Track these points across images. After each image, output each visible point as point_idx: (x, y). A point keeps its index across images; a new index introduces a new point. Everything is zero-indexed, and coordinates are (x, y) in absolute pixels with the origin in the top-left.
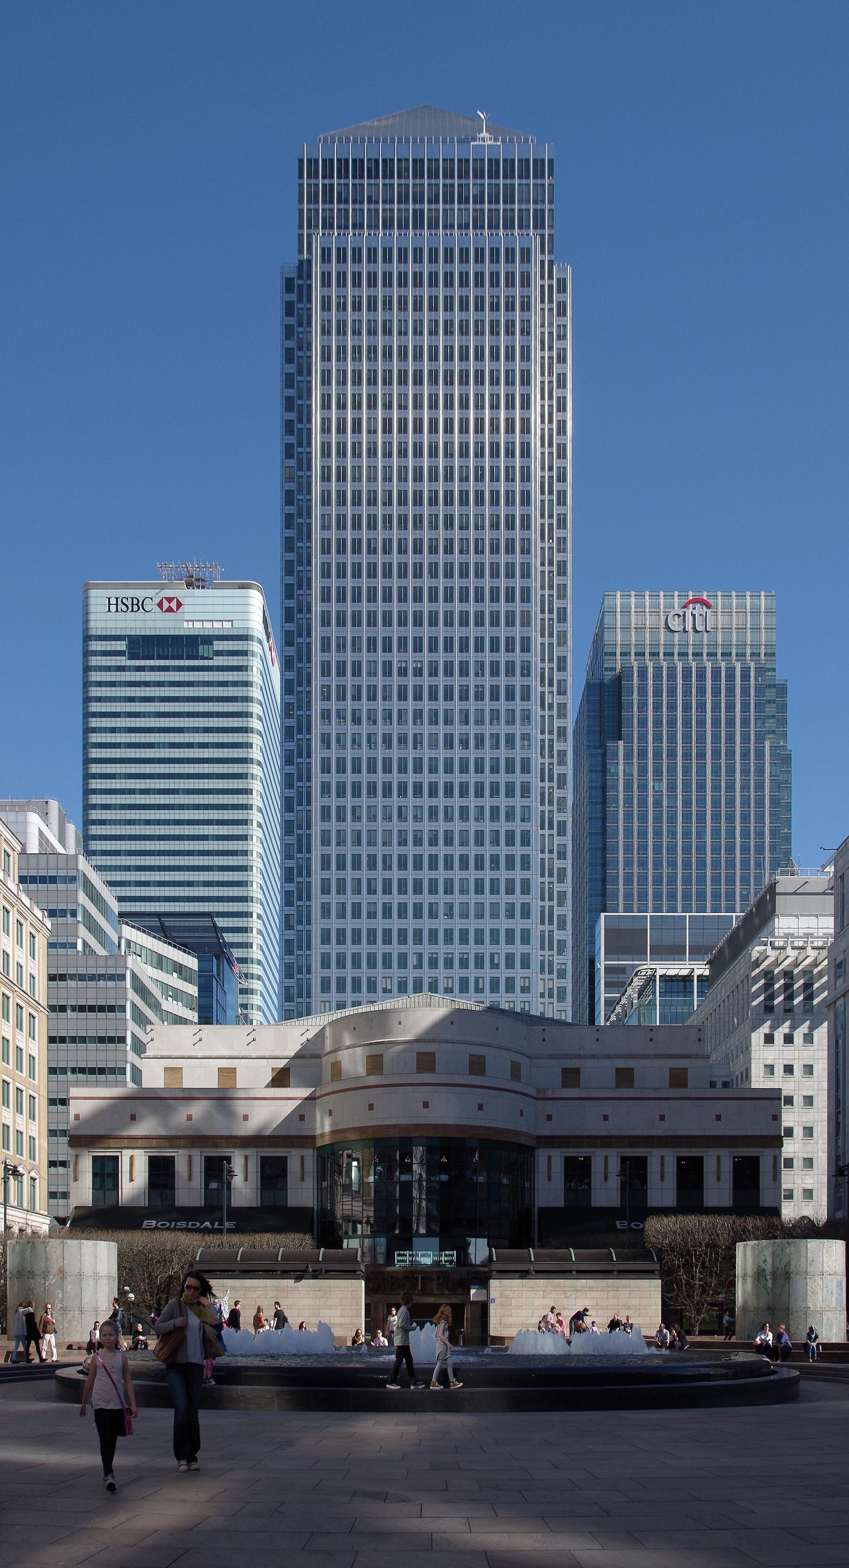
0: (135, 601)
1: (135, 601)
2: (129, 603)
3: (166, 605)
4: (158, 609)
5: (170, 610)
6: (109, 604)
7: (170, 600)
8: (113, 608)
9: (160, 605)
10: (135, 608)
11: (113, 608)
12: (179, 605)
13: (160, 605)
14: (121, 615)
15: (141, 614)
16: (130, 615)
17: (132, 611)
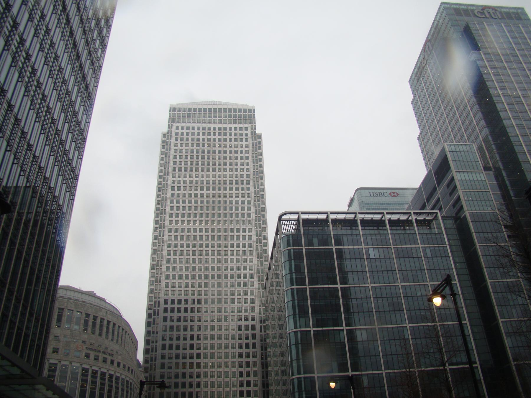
0: (380, 193)
1: (380, 193)
2: (378, 193)
3: (392, 194)
4: (390, 196)
5: (394, 196)
6: (370, 194)
7: (394, 193)
8: (372, 195)
9: (390, 194)
10: (381, 195)
11: (372, 195)
12: (398, 194)
13: (390, 194)
14: (375, 197)
15: (383, 197)
16: (379, 197)
17: (380, 196)
